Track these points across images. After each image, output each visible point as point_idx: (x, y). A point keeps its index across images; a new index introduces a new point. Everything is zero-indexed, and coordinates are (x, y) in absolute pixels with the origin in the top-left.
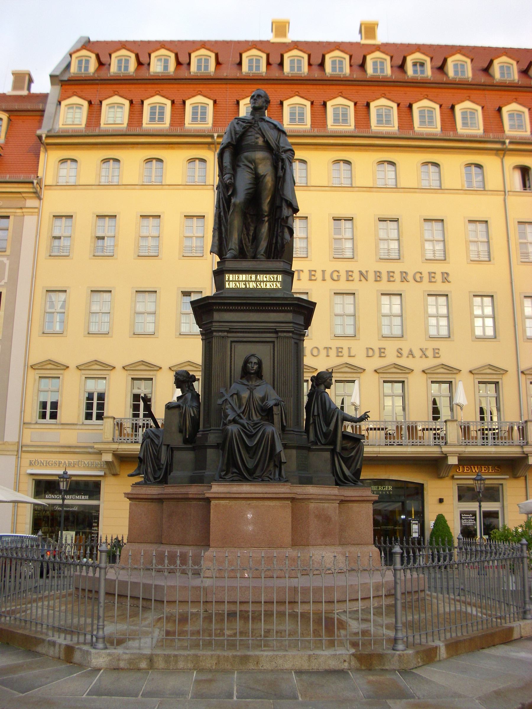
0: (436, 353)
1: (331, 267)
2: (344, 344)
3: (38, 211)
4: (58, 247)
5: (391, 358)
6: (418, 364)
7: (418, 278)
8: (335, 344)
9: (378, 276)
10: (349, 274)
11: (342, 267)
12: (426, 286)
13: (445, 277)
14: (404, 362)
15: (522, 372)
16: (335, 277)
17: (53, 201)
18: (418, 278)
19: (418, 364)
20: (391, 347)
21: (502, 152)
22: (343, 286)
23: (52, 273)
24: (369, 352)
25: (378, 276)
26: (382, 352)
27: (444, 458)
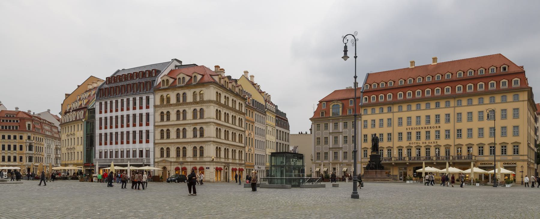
0: (437, 142)
1: (415, 127)
2: (418, 142)
3: (361, 120)
4: (365, 127)
5: (427, 144)
6: (433, 145)
7: (433, 127)
8: (416, 142)
9: (425, 128)
10: (419, 128)
11: (418, 126)
12: (436, 129)
13: (439, 127)
14: (430, 144)
15: (455, 145)
16: (416, 128)
17: (364, 118)
18: (433, 127)
19: (433, 145)
20: (427, 142)
21: (455, 98)
22: (418, 130)
23: (365, 132)
24: (423, 143)
25: (425, 128)
26: (425, 143)
27: (433, 163)
